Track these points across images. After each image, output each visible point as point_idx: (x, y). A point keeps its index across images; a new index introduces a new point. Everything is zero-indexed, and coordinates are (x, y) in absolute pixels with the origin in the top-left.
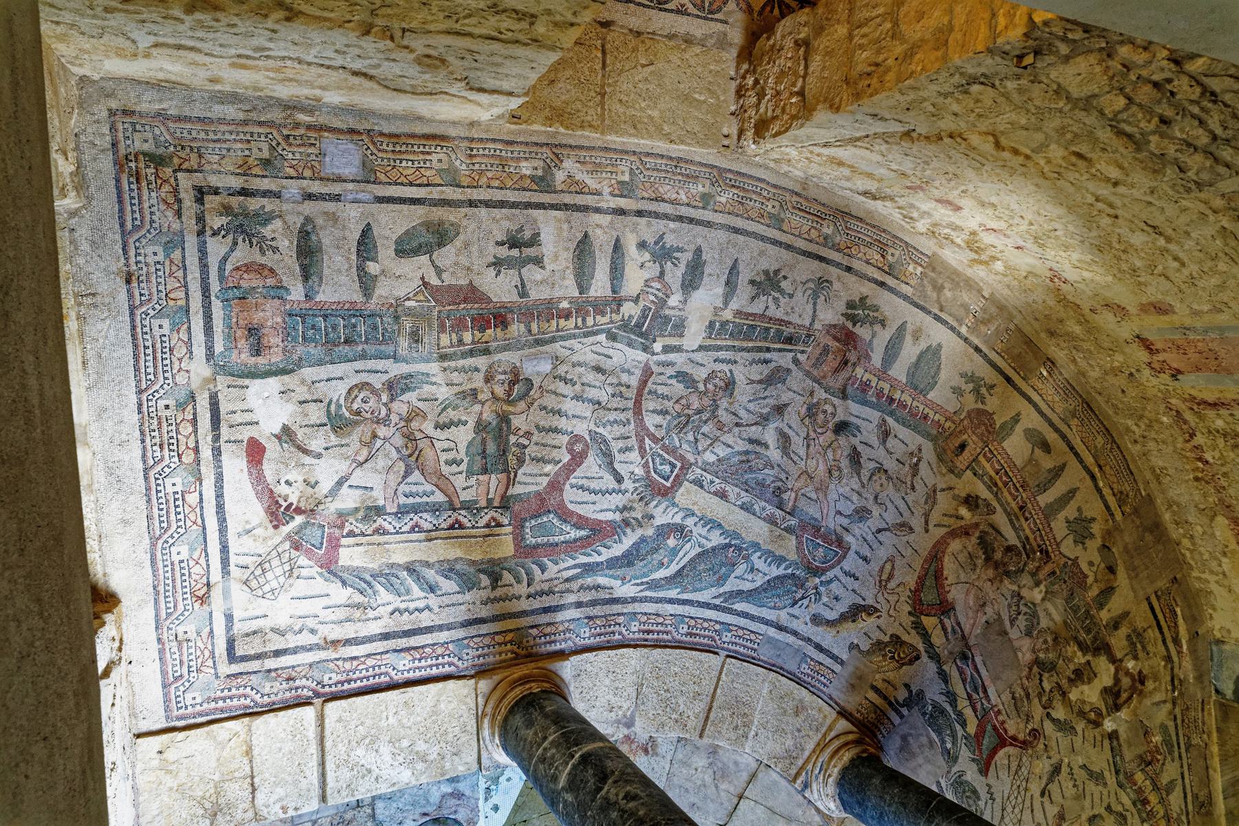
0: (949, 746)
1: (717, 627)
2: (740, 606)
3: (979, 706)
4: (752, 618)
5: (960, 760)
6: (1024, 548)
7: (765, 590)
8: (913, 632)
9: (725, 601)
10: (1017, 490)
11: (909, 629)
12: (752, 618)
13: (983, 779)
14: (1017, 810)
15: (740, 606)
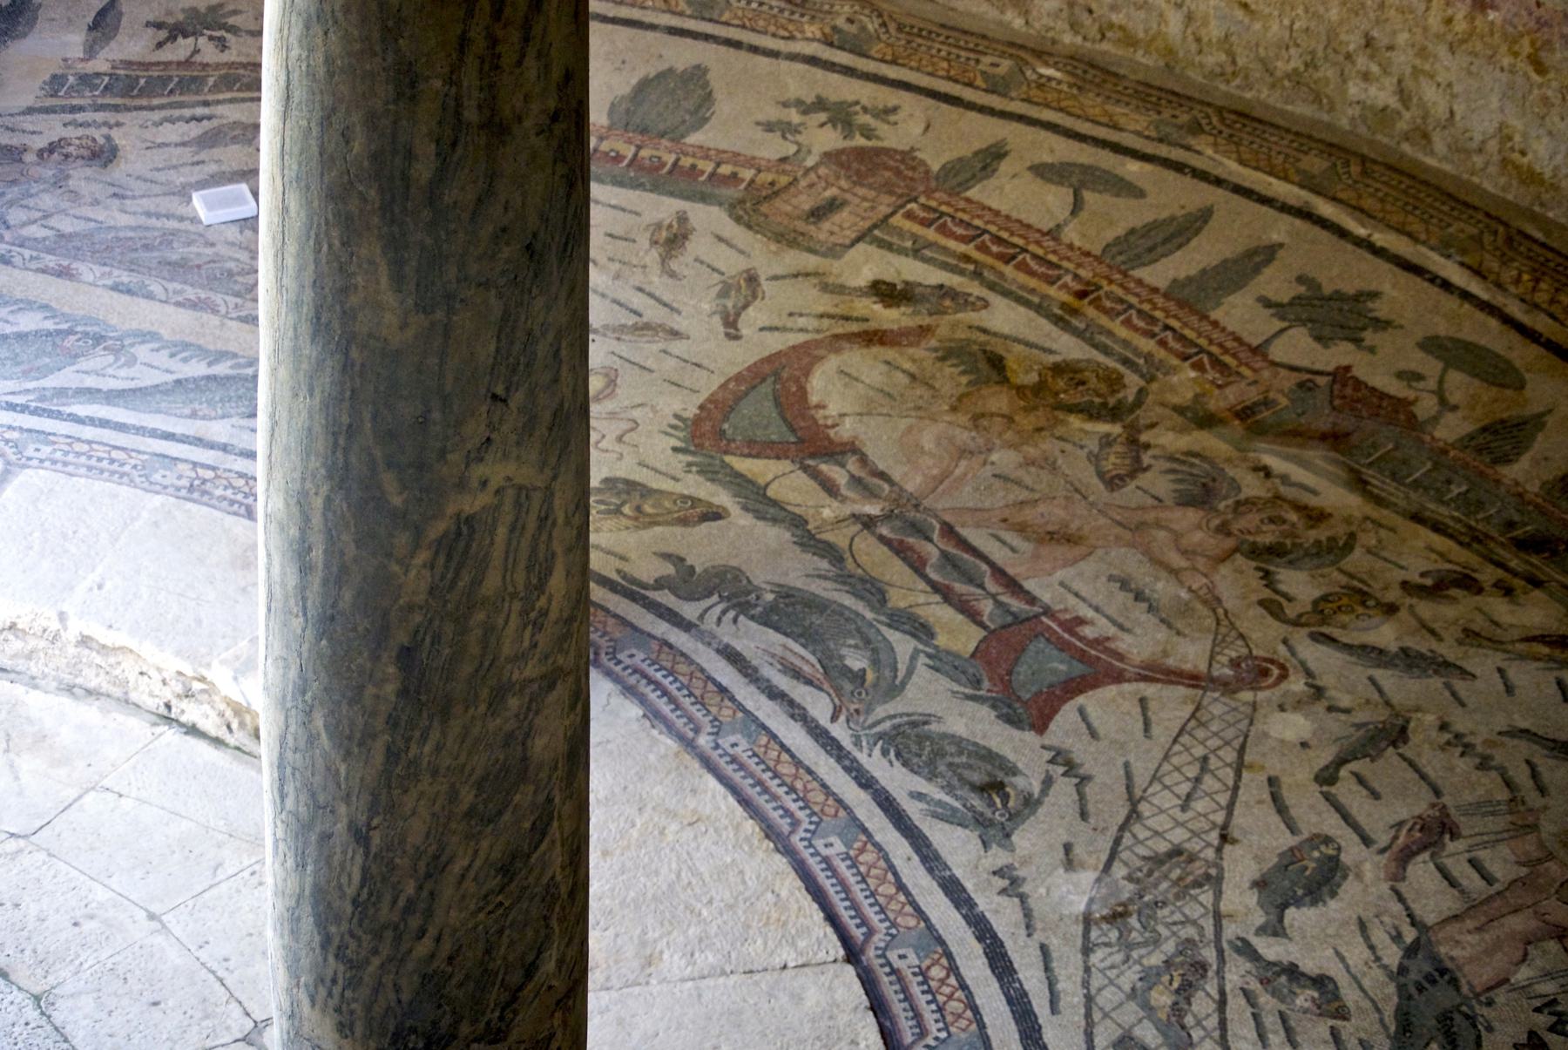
0: (856, 662)
1: (15, 435)
2: (81, 410)
3: (987, 607)
4: (121, 427)
5: (910, 691)
6: (1126, 362)
7: (166, 393)
8: (692, 478)
9: (42, 399)
10: (1058, 267)
11: (680, 475)
12: (121, 427)
13: (1030, 736)
14: (1199, 805)
15: (81, 410)
